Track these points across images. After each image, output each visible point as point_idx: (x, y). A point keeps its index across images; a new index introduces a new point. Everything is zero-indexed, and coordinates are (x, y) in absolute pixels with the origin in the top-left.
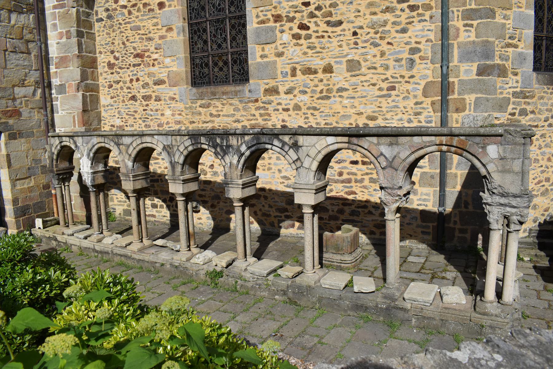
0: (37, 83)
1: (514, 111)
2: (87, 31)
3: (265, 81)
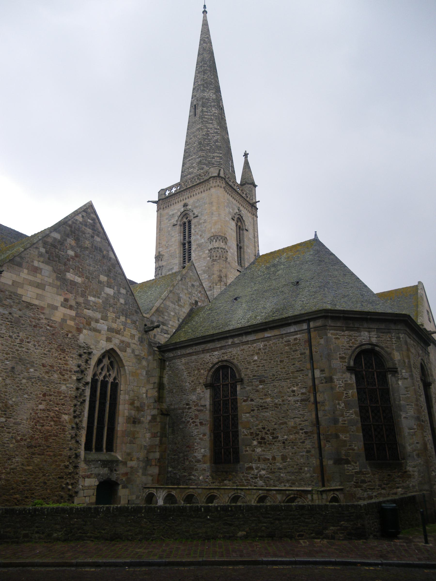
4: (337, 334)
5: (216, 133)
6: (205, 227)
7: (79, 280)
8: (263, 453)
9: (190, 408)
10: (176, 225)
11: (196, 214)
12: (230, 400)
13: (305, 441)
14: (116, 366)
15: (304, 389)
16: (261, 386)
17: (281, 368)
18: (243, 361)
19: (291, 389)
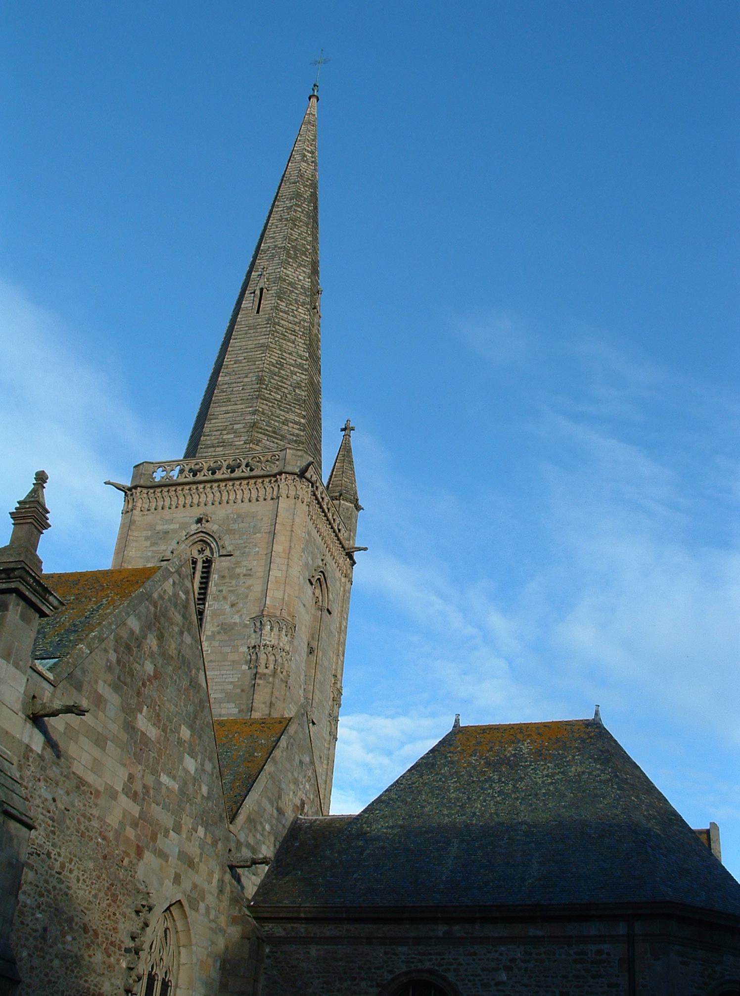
5: (301, 366)
6: (249, 587)
7: (153, 732)
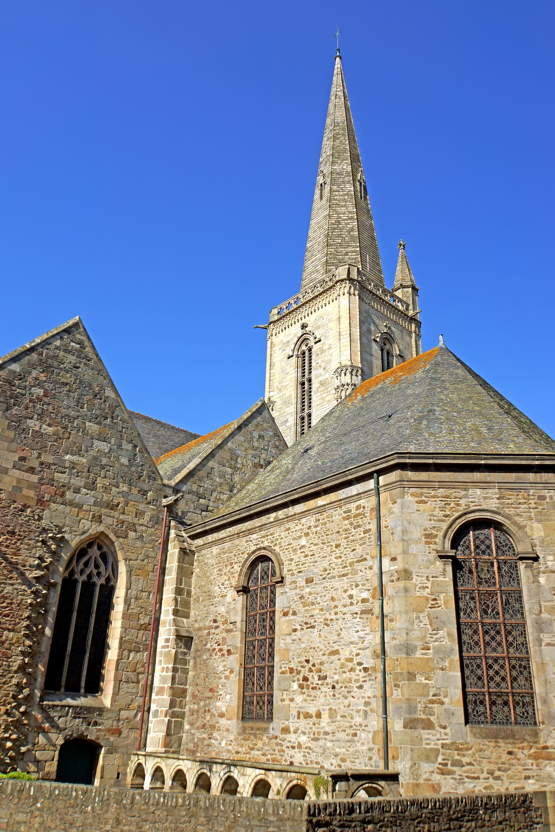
0: (139, 707)
1: (446, 761)
2: (182, 667)
3: (282, 722)
4: (422, 494)
5: (352, 218)
6: (331, 355)
8: (304, 704)
9: (217, 627)
10: (292, 356)
11: (318, 337)
12: (268, 613)
13: (364, 684)
14: (110, 560)
15: (367, 592)
16: (308, 590)
17: (336, 558)
18: (287, 547)
19: (348, 593)
